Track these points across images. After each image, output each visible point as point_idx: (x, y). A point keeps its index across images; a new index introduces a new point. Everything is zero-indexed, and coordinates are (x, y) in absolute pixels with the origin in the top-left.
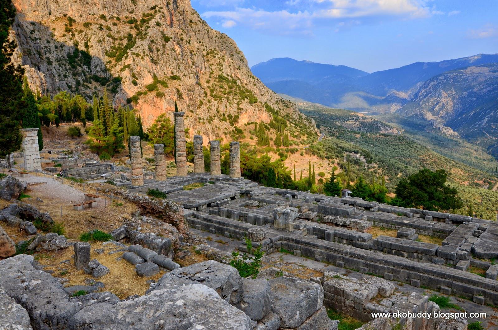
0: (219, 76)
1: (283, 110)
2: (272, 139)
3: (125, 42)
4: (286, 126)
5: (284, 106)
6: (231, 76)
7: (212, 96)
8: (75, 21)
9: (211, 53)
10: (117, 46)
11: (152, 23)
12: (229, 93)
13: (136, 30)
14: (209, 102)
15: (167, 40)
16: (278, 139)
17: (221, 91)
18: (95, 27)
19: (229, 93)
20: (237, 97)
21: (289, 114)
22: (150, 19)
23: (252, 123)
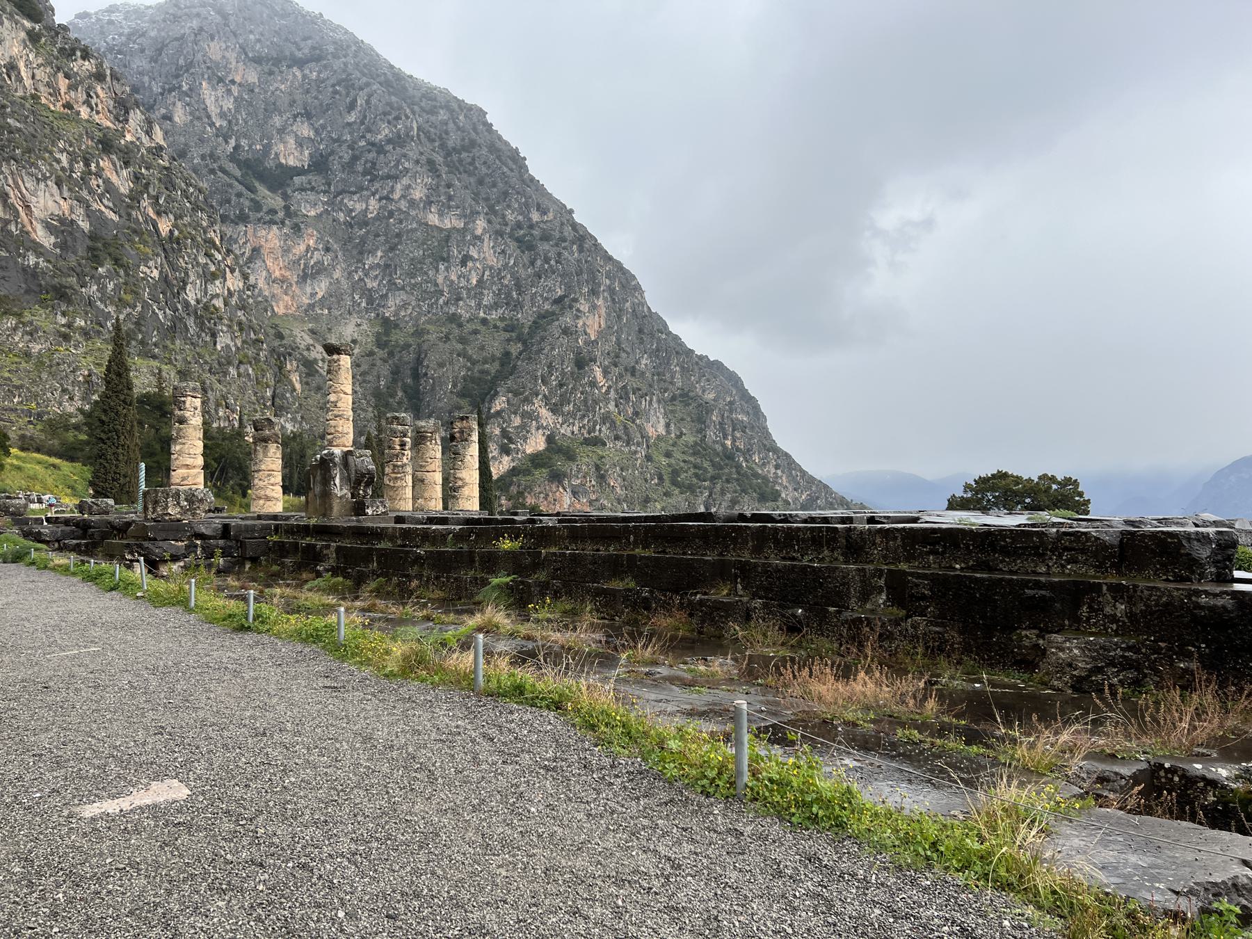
0: (696, 443)
3: (493, 368)
6: (723, 445)
7: (674, 483)
8: (396, 326)
9: (681, 395)
10: (477, 375)
11: (555, 329)
12: (713, 478)
13: (519, 345)
14: (667, 494)
15: (581, 363)
17: (696, 475)
18: (432, 337)
19: (713, 478)
20: (733, 486)
22: (549, 323)
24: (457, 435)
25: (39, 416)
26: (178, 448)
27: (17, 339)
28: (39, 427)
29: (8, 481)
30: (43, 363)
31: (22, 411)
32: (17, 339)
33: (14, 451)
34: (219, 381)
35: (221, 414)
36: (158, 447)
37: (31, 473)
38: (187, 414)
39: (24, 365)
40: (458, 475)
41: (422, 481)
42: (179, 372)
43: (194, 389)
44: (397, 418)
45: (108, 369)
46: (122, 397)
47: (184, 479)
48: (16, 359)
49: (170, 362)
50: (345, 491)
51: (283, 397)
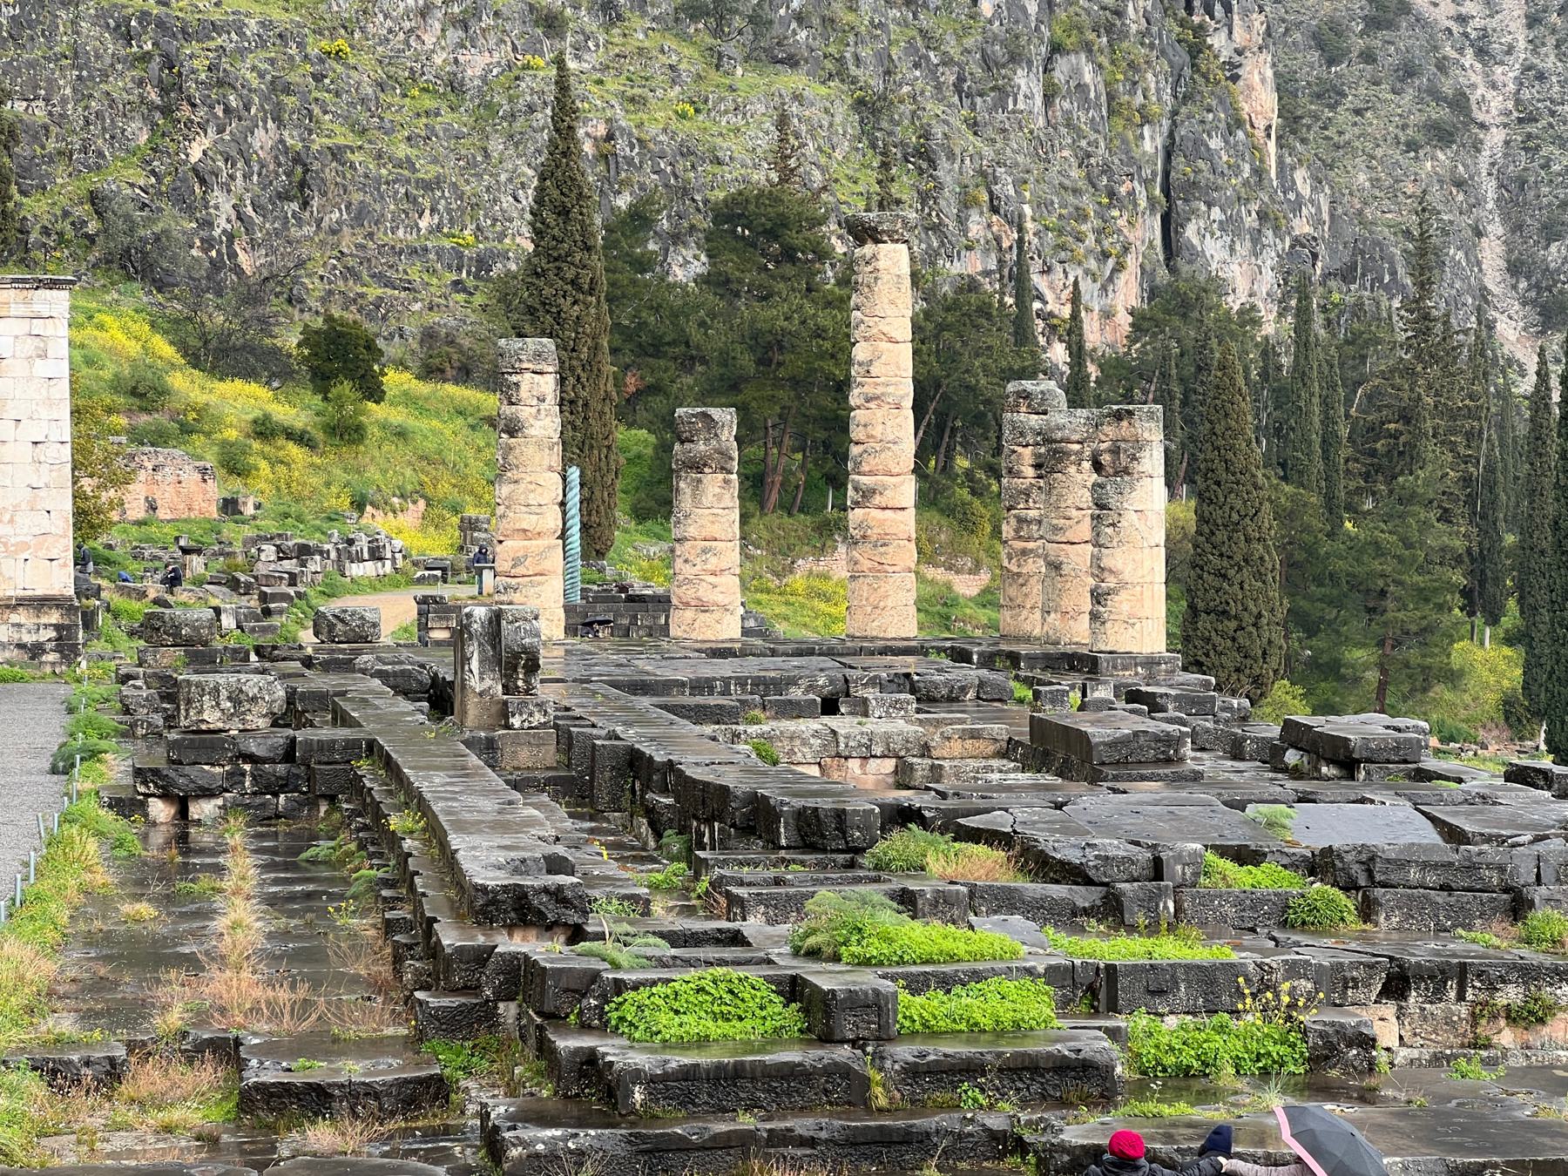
24: (1106, 459)
25: (483, 264)
27: (430, 39)
28: (479, 299)
29: (373, 473)
30: (489, 106)
31: (440, 253)
32: (430, 39)
33: (395, 380)
34: (974, 126)
35: (976, 228)
36: (746, 362)
37: (430, 446)
38: (524, 413)
39: (447, 117)
42: (860, 104)
43: (538, 355)
44: (1026, 395)
45: (539, 201)
46: (570, 274)
47: (517, 562)
48: (429, 103)
49: (841, 73)
50: (488, 683)
51: (1198, 149)
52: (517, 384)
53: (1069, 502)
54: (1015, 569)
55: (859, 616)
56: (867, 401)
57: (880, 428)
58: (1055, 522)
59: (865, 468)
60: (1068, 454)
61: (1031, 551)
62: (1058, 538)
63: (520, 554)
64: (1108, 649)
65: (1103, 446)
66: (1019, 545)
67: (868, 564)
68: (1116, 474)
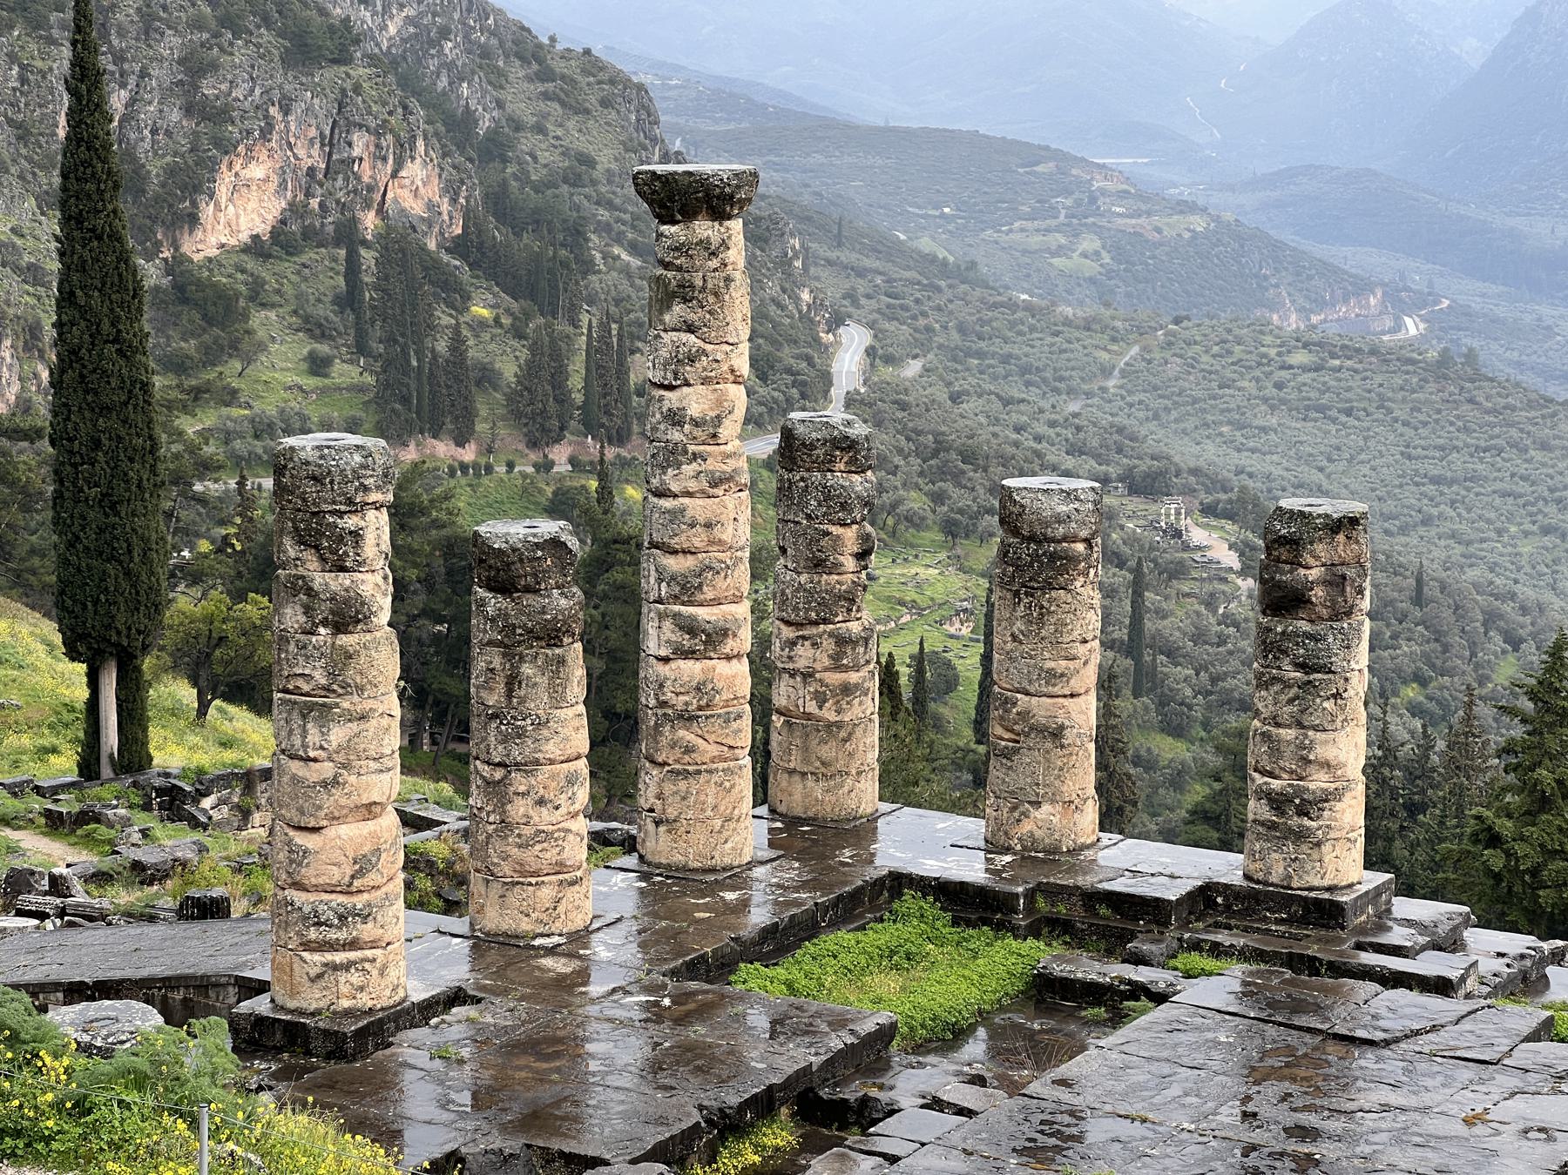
1: (540, 129)
2: (487, 377)
4: (588, 267)
5: (546, 96)
16: (545, 366)
21: (589, 162)
23: (311, 236)
24: (1318, 594)
26: (338, 734)
40: (1320, 752)
41: (1057, 734)
52: (357, 535)
53: (1076, 633)
54: (831, 716)
55: (699, 836)
56: (714, 484)
57: (730, 529)
58: (1049, 665)
59: (709, 594)
60: (1073, 559)
61: (857, 686)
62: (1056, 690)
63: (366, 849)
64: (1326, 883)
65: (1314, 574)
66: (834, 678)
67: (713, 750)
68: (1336, 616)
